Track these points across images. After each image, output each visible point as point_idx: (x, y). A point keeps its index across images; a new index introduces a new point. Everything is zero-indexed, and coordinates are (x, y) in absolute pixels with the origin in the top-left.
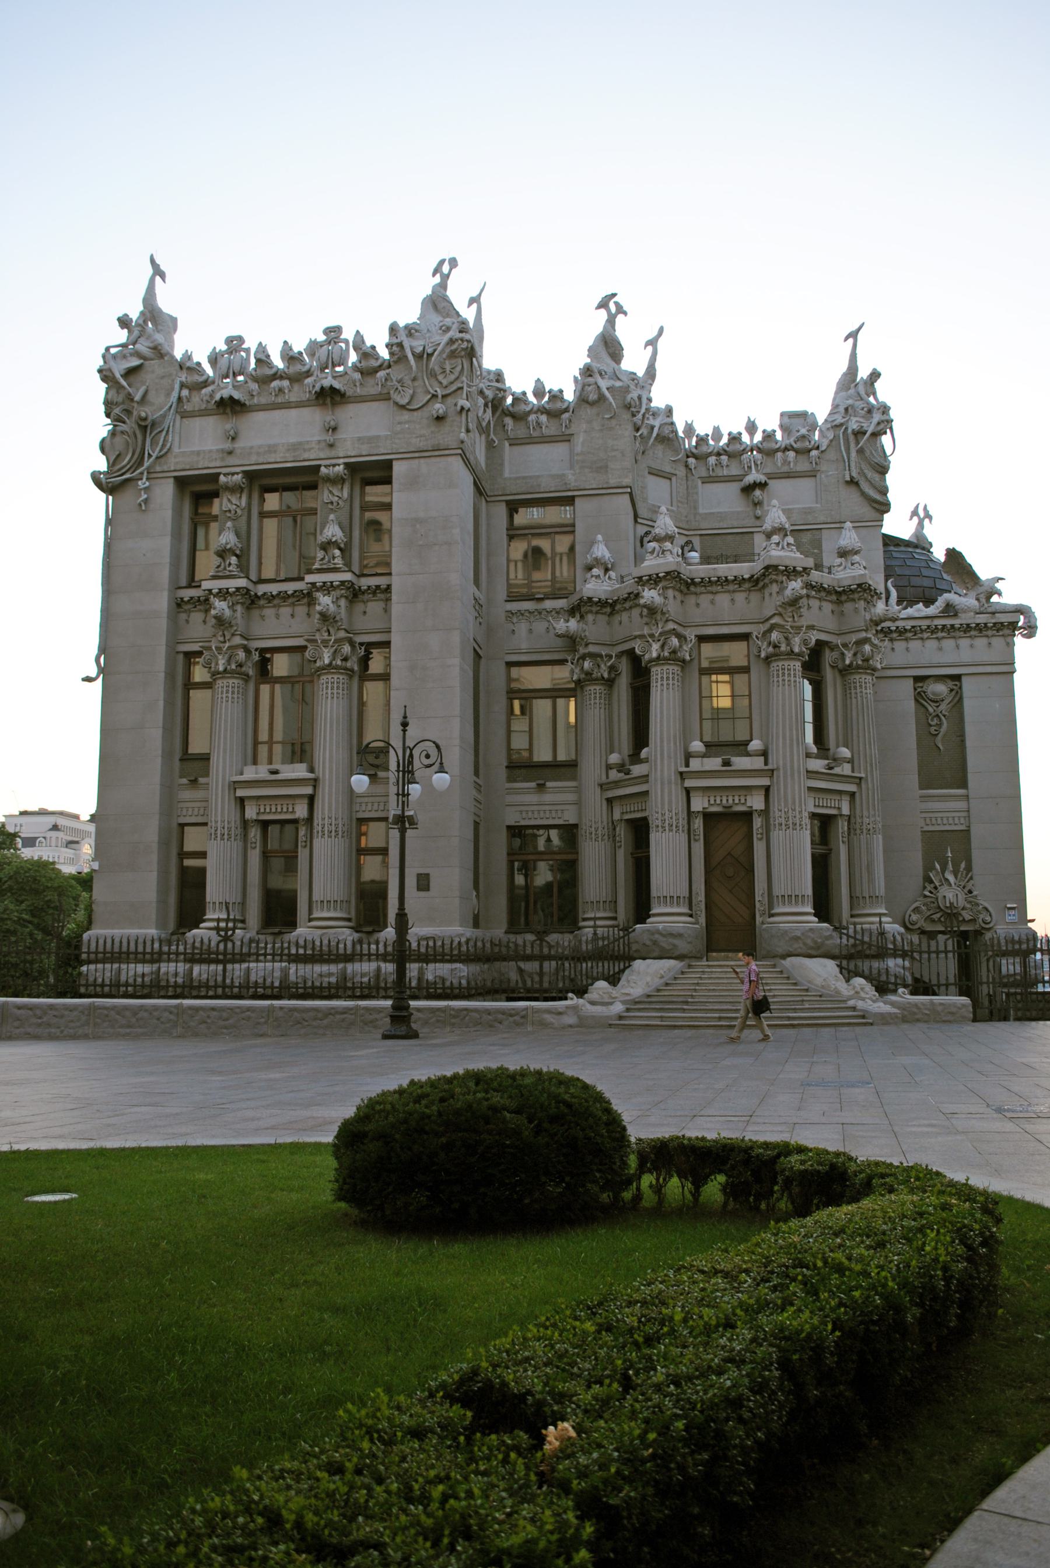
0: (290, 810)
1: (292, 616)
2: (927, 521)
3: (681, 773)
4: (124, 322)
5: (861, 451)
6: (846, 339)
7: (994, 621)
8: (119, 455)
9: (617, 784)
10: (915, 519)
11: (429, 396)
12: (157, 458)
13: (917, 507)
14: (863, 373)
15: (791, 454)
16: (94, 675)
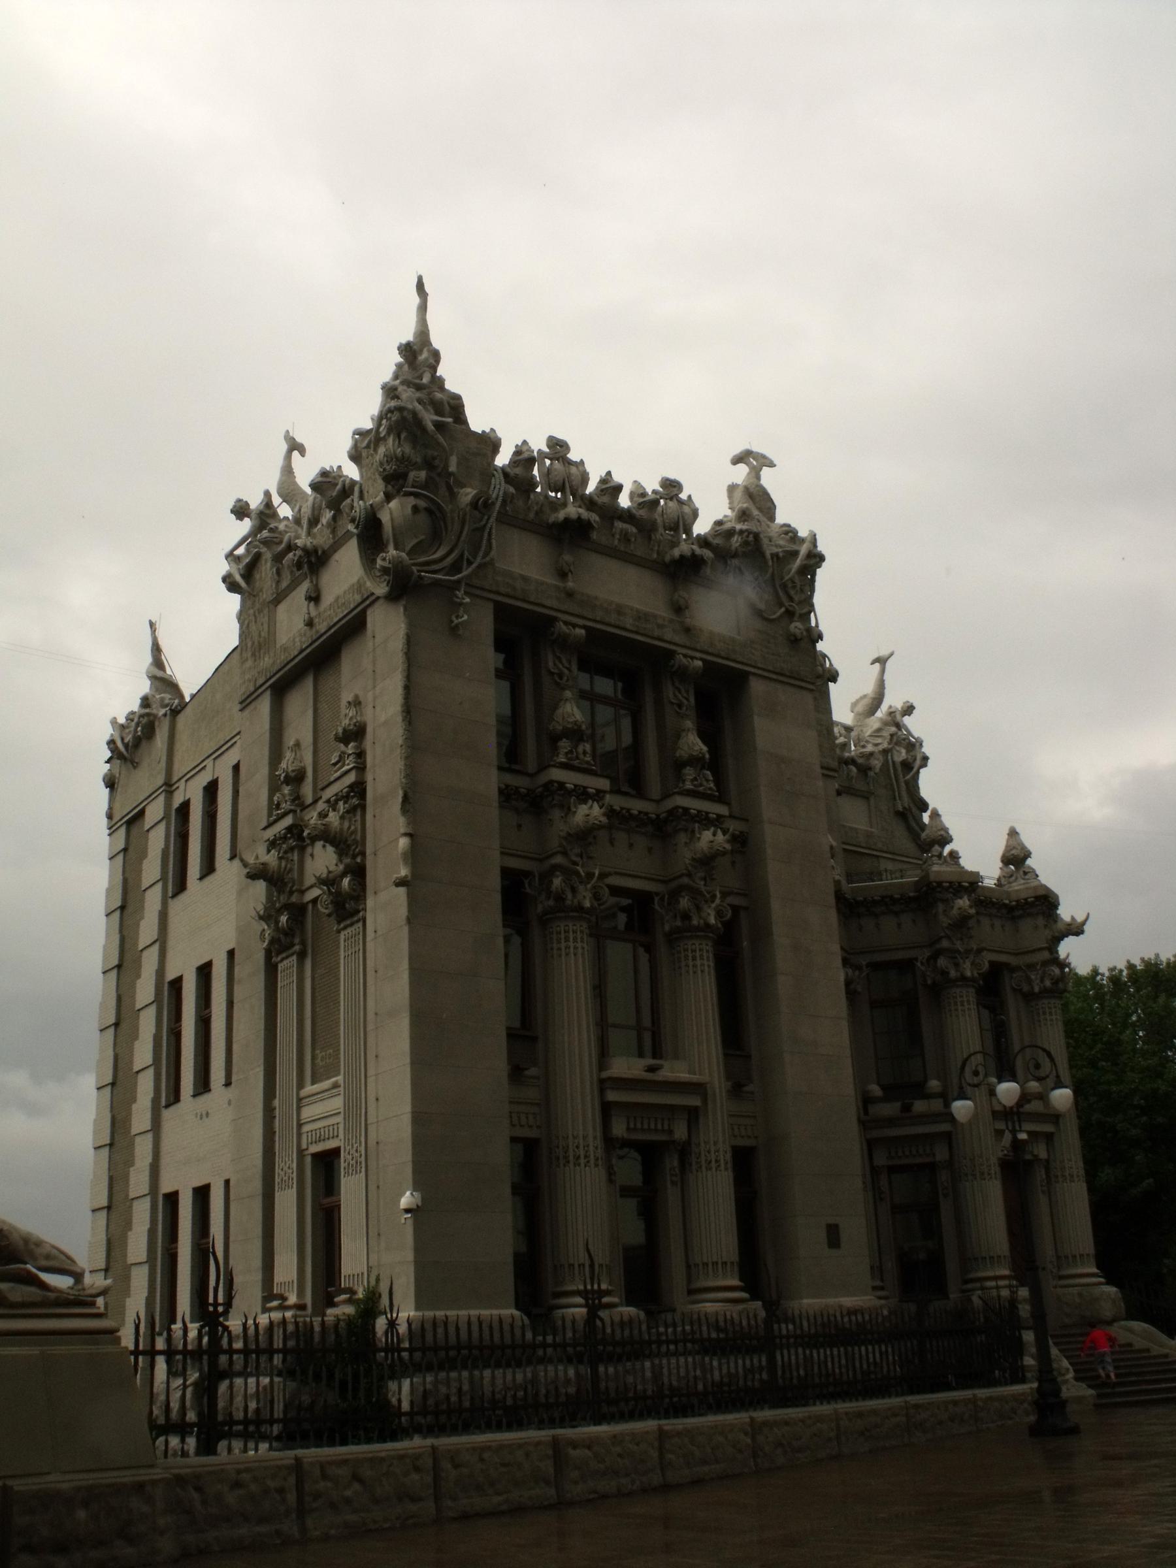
0: (666, 1127)
1: (631, 845)
5: (907, 783)
6: (872, 663)
8: (421, 541)
9: (891, 1122)
11: (783, 609)
12: (480, 566)
14: (893, 700)
15: (854, 769)
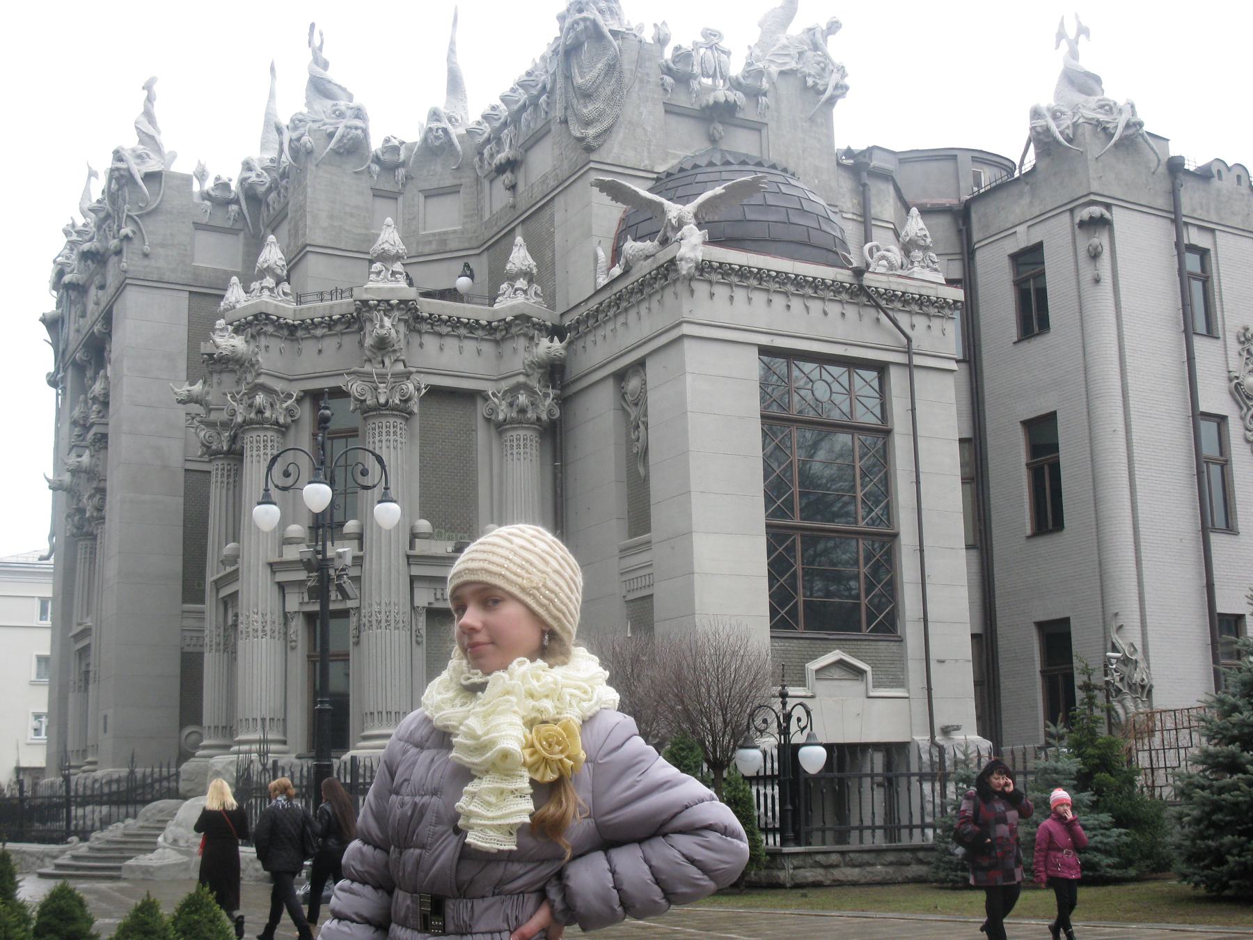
2: (1082, 37)
3: (216, 582)
4: (67, 233)
7: (655, 266)
10: (1064, 42)
13: (1062, 24)
16: (46, 553)
